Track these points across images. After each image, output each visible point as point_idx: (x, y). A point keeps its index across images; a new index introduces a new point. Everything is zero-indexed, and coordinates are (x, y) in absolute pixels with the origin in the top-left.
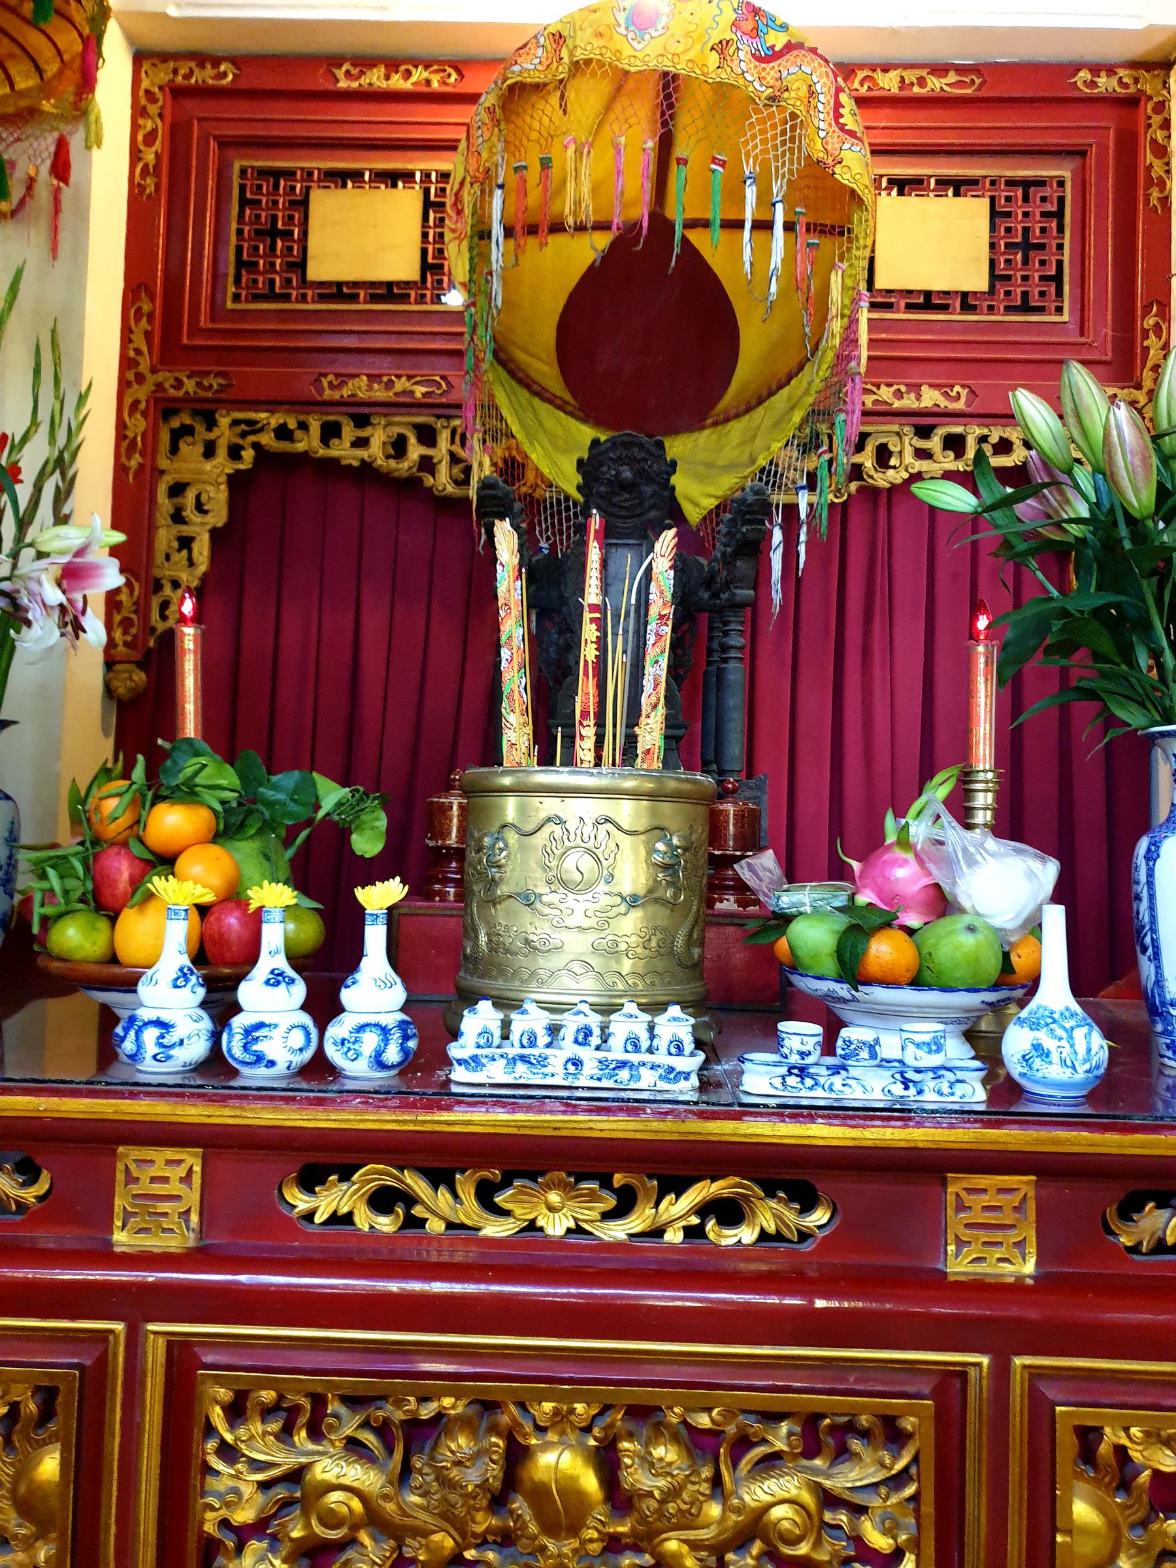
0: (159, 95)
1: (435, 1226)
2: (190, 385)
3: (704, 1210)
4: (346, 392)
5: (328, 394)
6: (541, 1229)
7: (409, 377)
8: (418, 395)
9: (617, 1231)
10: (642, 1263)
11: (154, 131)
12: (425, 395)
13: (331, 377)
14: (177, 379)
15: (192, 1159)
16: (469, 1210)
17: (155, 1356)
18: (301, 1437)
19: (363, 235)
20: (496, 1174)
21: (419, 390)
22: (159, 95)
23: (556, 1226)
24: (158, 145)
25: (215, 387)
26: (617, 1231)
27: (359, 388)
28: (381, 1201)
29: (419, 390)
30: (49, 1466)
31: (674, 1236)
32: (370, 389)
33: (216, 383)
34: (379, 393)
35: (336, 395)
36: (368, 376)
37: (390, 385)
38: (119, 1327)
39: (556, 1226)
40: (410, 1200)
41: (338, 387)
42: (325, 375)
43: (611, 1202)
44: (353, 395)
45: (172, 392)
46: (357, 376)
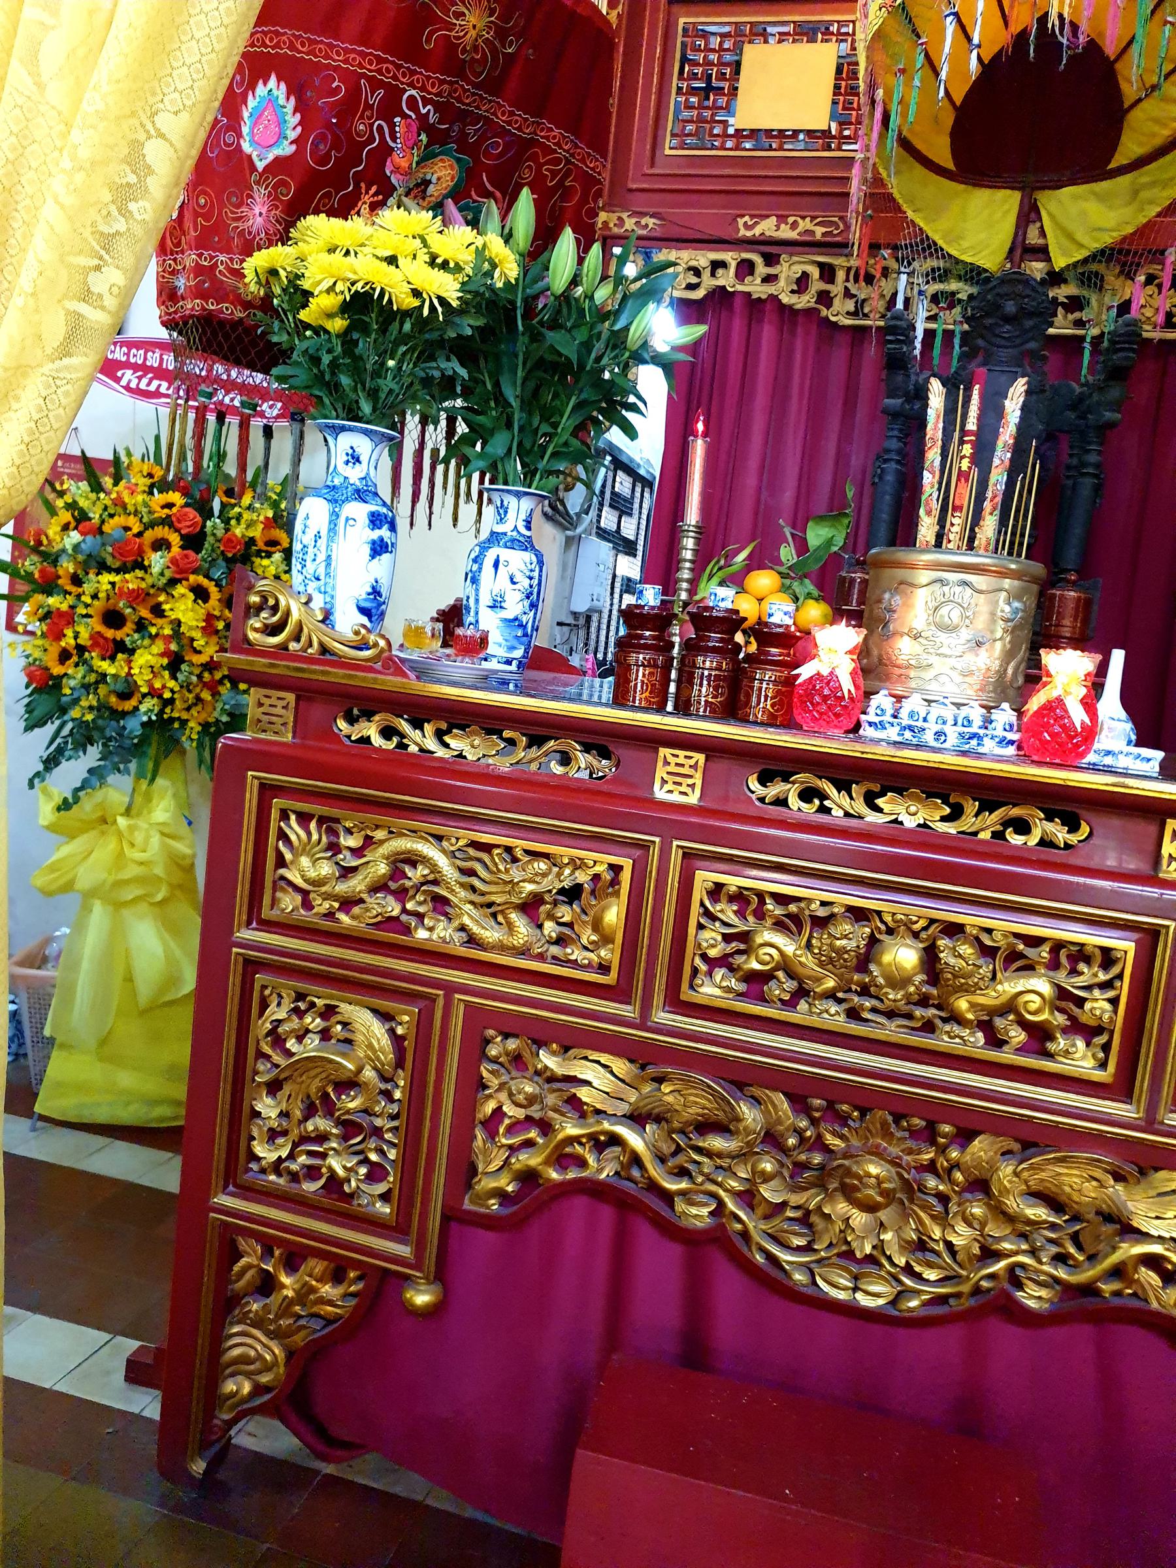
1: (837, 812)
2: (630, 223)
3: (1007, 823)
4: (757, 231)
5: (743, 232)
6: (901, 823)
7: (813, 218)
8: (818, 236)
9: (950, 828)
10: (966, 844)
12: (824, 234)
13: (747, 218)
14: (620, 219)
15: (700, 758)
16: (860, 807)
17: (676, 857)
18: (751, 919)
20: (877, 788)
21: (819, 231)
23: (910, 823)
26: (950, 828)
27: (767, 227)
28: (807, 795)
29: (819, 231)
30: (614, 915)
31: (985, 835)
32: (778, 228)
33: (651, 222)
34: (786, 233)
35: (749, 234)
37: (794, 226)
38: (657, 840)
39: (910, 823)
40: (823, 796)
42: (743, 216)
43: (948, 810)
45: (616, 230)
46: (768, 216)
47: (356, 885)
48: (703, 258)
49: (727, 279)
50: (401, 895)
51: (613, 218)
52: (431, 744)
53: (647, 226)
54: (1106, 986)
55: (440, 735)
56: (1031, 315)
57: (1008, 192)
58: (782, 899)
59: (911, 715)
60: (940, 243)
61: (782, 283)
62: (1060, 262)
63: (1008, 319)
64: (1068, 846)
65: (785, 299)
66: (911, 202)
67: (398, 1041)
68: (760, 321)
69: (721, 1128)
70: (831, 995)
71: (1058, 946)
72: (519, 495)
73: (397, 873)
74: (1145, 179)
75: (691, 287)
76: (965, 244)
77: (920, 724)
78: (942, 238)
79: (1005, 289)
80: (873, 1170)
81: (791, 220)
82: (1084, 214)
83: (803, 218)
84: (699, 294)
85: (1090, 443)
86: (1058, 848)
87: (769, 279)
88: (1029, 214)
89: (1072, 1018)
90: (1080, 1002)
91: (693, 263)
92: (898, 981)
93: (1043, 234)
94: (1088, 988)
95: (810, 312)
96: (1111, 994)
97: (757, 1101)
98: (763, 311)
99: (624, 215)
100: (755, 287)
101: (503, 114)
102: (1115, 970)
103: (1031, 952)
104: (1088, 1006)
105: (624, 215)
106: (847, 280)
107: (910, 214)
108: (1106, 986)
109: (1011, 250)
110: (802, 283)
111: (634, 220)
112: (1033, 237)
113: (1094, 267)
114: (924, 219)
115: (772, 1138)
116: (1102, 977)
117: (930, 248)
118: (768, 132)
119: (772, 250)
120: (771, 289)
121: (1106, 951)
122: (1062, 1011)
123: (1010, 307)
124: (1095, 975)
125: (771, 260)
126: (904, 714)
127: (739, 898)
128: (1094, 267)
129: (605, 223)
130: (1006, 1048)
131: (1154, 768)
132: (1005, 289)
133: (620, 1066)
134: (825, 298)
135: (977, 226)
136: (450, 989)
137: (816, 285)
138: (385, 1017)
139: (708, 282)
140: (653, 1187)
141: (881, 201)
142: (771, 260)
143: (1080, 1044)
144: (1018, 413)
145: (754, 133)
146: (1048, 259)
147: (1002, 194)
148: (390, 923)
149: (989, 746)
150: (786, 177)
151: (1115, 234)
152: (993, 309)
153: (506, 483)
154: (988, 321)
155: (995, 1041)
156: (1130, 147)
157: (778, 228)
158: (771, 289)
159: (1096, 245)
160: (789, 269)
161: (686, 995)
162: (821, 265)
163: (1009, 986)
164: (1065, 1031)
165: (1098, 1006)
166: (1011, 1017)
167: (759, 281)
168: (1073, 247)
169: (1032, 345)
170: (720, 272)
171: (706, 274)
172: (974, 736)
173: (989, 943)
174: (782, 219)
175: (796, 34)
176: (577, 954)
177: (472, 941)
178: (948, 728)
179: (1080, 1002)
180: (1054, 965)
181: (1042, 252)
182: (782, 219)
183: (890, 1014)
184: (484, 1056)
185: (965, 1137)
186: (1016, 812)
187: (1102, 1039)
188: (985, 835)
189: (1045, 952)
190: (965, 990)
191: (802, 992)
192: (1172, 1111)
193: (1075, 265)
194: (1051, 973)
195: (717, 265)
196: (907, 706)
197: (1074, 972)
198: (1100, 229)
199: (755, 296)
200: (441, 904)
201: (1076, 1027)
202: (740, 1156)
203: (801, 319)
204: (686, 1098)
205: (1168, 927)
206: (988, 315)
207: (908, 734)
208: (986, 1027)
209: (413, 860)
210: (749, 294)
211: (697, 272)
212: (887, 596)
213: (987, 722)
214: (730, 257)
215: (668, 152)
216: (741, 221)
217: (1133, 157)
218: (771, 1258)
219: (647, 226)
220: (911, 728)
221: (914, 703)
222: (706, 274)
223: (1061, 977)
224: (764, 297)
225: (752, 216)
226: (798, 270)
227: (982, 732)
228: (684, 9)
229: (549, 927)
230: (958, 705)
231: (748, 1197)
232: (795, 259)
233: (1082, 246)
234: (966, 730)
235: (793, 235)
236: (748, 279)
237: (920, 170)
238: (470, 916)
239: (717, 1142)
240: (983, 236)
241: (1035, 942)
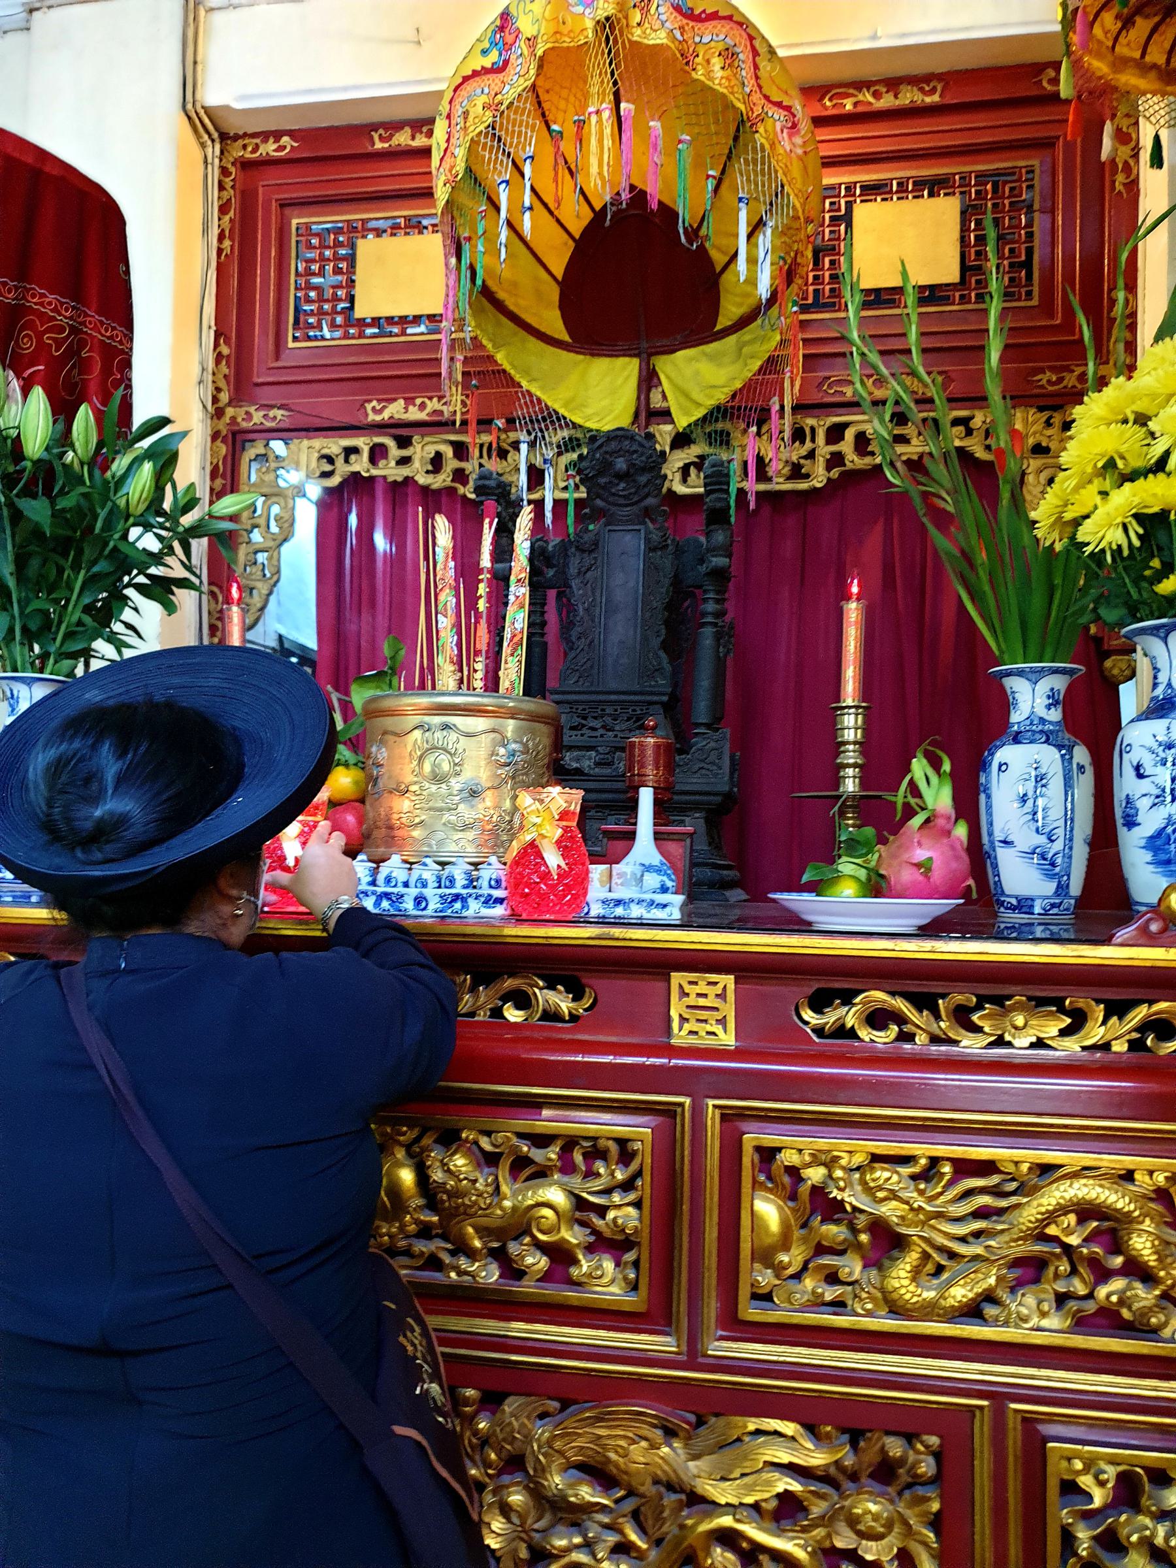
0: (233, 170)
2: (258, 417)
4: (386, 415)
5: (372, 417)
11: (229, 200)
13: (374, 403)
14: (247, 413)
19: (403, 277)
22: (233, 170)
24: (232, 214)
25: (279, 417)
32: (406, 409)
33: (279, 413)
34: (414, 414)
35: (378, 418)
36: (405, 399)
37: (422, 406)
41: (380, 411)
42: (370, 401)
44: (391, 417)
46: (395, 400)
48: (335, 445)
49: (360, 464)
51: (240, 413)
53: (275, 418)
54: (627, 1186)
56: (643, 470)
57: (627, 359)
59: (388, 880)
60: (562, 411)
61: (417, 464)
62: (682, 421)
63: (621, 477)
64: (574, 1018)
65: (422, 480)
66: (526, 372)
68: (404, 504)
71: (570, 1143)
72: (29, 682)
74: (747, 337)
75: (326, 475)
76: (589, 411)
77: (400, 889)
78: (565, 406)
79: (613, 445)
81: (418, 401)
82: (697, 373)
83: (430, 398)
84: (335, 481)
85: (705, 592)
86: (562, 1020)
87: (404, 461)
88: (648, 380)
89: (595, 1232)
90: (602, 1211)
91: (325, 451)
93: (665, 397)
94: (607, 1192)
95: (451, 491)
96: (632, 1197)
98: (407, 495)
99: (252, 409)
100: (390, 470)
101: (9, 291)
102: (634, 1166)
103: (537, 1155)
104: (611, 1215)
105: (252, 409)
106: (481, 456)
107: (524, 384)
108: (627, 1186)
109: (637, 415)
110: (437, 462)
111: (262, 413)
112: (656, 401)
113: (720, 426)
114: (542, 388)
116: (619, 1176)
117: (553, 418)
118: (390, 320)
119: (403, 432)
120: (405, 471)
121: (622, 1142)
122: (583, 1224)
123: (621, 464)
124: (612, 1174)
125: (404, 442)
126: (381, 878)
128: (720, 426)
129: (233, 419)
130: (524, 1282)
131: (676, 915)
132: (613, 445)
134: (460, 476)
135: (598, 393)
137: (451, 464)
139: (342, 470)
141: (485, 375)
142: (404, 442)
143: (609, 1265)
144: (527, 544)
145: (376, 321)
146: (673, 422)
147: (622, 361)
149: (474, 907)
150: (403, 361)
151: (726, 390)
152: (605, 467)
153: (15, 670)
154: (602, 481)
156: (730, 311)
157: (406, 409)
158: (405, 471)
159: (711, 402)
160: (422, 450)
162: (452, 443)
164: (590, 1249)
165: (624, 1215)
166: (527, 1240)
167: (393, 463)
168: (689, 404)
169: (650, 501)
170: (353, 457)
171: (340, 461)
172: (457, 897)
173: (488, 1147)
174: (409, 401)
175: (406, 227)
178: (430, 892)
179: (602, 1211)
180: (568, 1168)
181: (665, 415)
182: (409, 401)
186: (509, 983)
187: (630, 1256)
188: (482, 1016)
189: (552, 1153)
192: (722, 1338)
193: (696, 423)
194: (566, 1179)
195: (350, 451)
196: (385, 870)
197: (591, 1174)
198: (714, 387)
199: (390, 479)
201: (600, 1244)
203: (444, 499)
205: (682, 1105)
206: (600, 473)
207: (385, 904)
208: (500, 1255)
210: (385, 477)
211: (330, 460)
212: (374, 749)
213: (471, 882)
214: (363, 443)
215: (291, 345)
216: (369, 407)
217: (735, 318)
219: (275, 418)
220: (387, 895)
221: (394, 866)
222: (340, 461)
223: (576, 1181)
224: (400, 479)
225: (379, 401)
226: (431, 450)
227: (464, 892)
228: (296, 211)
230: (443, 864)
232: (427, 439)
233: (699, 405)
234: (448, 891)
235: (422, 416)
236: (382, 463)
237: (533, 343)
240: (606, 402)
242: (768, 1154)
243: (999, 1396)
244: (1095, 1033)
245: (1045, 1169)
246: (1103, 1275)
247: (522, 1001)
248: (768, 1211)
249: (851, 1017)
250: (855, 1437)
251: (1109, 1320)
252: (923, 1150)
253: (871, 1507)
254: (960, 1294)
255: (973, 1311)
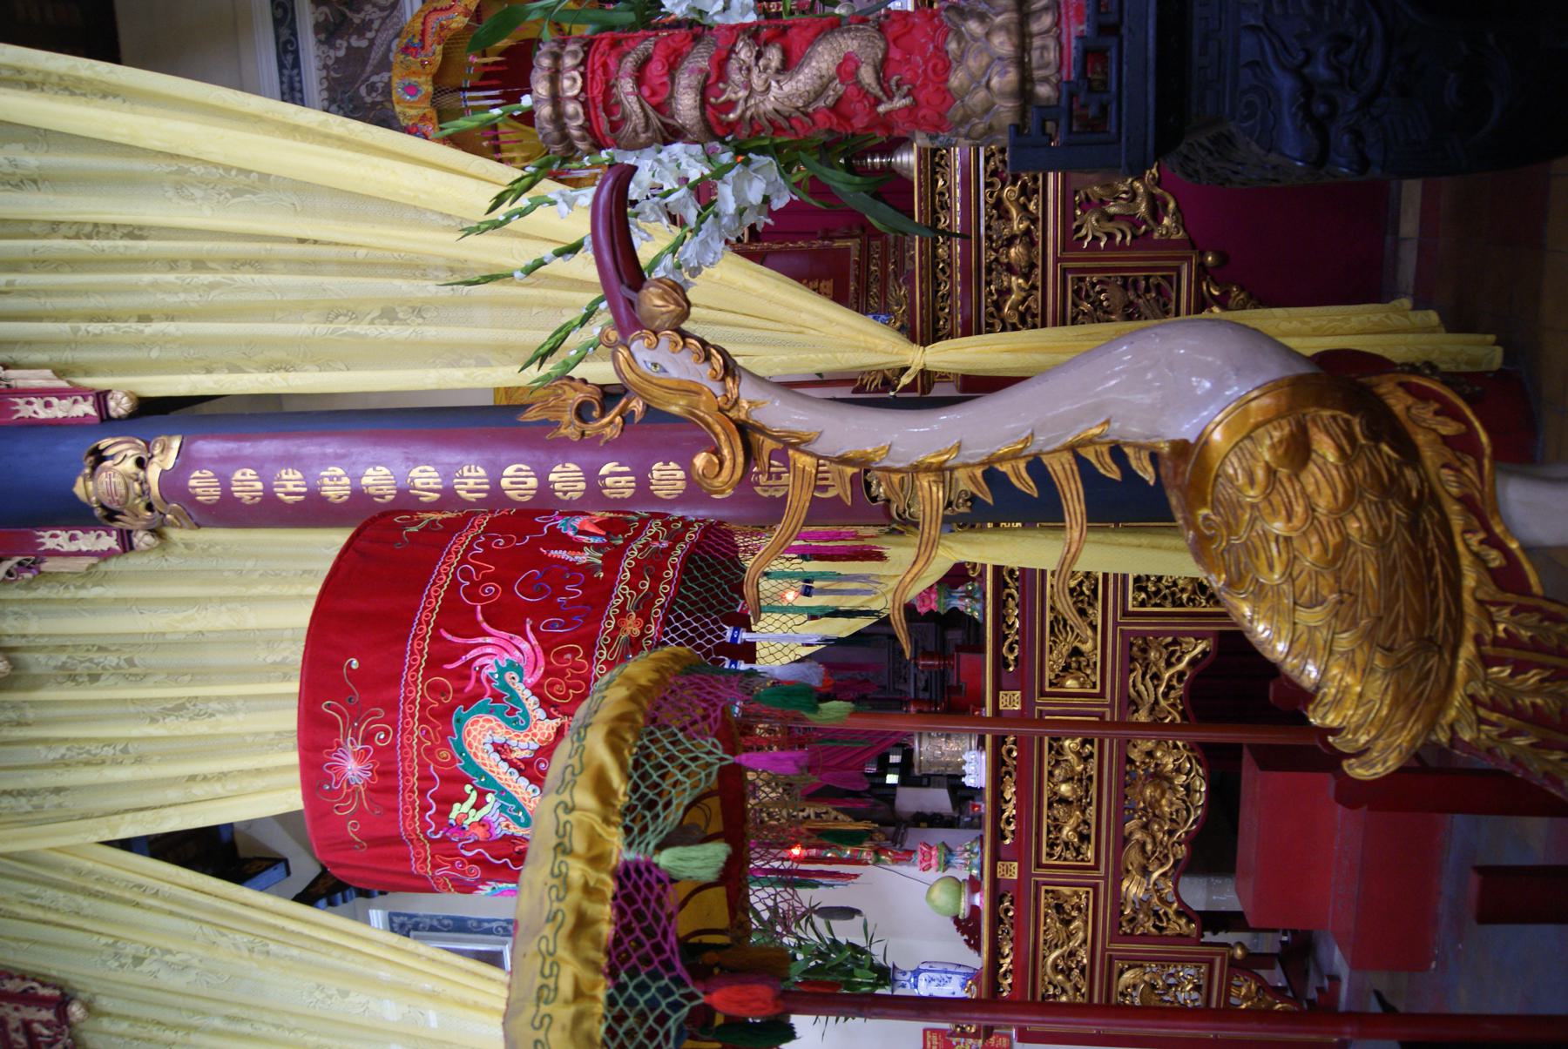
16: (1011, 805)
30: (1066, 890)
47: (1068, 986)
50: (1071, 969)
52: (1008, 960)
55: (1004, 957)
58: (1049, 832)
67: (1130, 968)
69: (1143, 845)
70: (1083, 812)
73: (1062, 971)
80: (1148, 792)
92: (1074, 790)
97: (1131, 834)
115: (1145, 827)
127: (1051, 845)
133: (1125, 884)
136: (1104, 950)
138: (1121, 972)
140: (1174, 866)
148: (1082, 971)
155: (1091, 755)
161: (1092, 863)
163: (1071, 757)
176: (1084, 902)
177: (1085, 941)
183: (1087, 791)
184: (1132, 934)
185: (1132, 762)
190: (1073, 770)
191: (1085, 822)
200: (1072, 954)
202: (1154, 838)
204: (1133, 857)
209: (1055, 966)
218: (1195, 822)
229: (1075, 913)
231: (1171, 833)
238: (1074, 944)
239: (1149, 847)
241: (1051, 747)
242: (1051, 684)
243: (1116, 624)
244: (1013, 591)
245: (1052, 609)
246: (1082, 593)
247: (1010, 751)
248: (1071, 684)
249: (1011, 657)
250: (1133, 659)
251: (1095, 591)
252: (1048, 644)
253: (1153, 655)
254: (1090, 632)
255: (1094, 628)
